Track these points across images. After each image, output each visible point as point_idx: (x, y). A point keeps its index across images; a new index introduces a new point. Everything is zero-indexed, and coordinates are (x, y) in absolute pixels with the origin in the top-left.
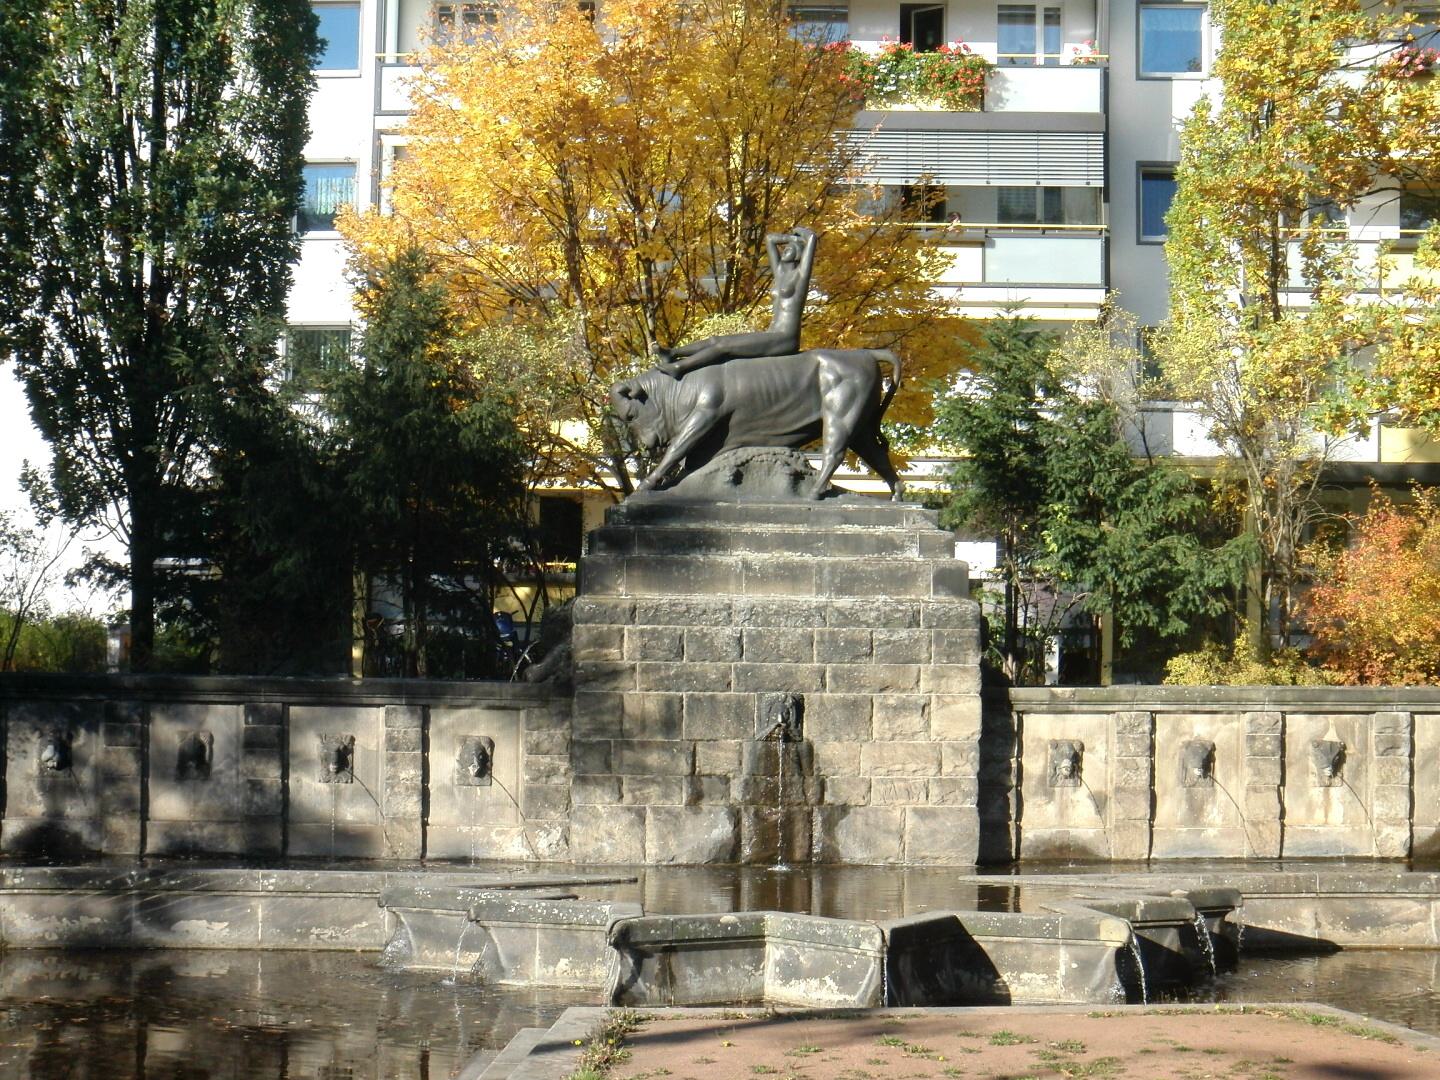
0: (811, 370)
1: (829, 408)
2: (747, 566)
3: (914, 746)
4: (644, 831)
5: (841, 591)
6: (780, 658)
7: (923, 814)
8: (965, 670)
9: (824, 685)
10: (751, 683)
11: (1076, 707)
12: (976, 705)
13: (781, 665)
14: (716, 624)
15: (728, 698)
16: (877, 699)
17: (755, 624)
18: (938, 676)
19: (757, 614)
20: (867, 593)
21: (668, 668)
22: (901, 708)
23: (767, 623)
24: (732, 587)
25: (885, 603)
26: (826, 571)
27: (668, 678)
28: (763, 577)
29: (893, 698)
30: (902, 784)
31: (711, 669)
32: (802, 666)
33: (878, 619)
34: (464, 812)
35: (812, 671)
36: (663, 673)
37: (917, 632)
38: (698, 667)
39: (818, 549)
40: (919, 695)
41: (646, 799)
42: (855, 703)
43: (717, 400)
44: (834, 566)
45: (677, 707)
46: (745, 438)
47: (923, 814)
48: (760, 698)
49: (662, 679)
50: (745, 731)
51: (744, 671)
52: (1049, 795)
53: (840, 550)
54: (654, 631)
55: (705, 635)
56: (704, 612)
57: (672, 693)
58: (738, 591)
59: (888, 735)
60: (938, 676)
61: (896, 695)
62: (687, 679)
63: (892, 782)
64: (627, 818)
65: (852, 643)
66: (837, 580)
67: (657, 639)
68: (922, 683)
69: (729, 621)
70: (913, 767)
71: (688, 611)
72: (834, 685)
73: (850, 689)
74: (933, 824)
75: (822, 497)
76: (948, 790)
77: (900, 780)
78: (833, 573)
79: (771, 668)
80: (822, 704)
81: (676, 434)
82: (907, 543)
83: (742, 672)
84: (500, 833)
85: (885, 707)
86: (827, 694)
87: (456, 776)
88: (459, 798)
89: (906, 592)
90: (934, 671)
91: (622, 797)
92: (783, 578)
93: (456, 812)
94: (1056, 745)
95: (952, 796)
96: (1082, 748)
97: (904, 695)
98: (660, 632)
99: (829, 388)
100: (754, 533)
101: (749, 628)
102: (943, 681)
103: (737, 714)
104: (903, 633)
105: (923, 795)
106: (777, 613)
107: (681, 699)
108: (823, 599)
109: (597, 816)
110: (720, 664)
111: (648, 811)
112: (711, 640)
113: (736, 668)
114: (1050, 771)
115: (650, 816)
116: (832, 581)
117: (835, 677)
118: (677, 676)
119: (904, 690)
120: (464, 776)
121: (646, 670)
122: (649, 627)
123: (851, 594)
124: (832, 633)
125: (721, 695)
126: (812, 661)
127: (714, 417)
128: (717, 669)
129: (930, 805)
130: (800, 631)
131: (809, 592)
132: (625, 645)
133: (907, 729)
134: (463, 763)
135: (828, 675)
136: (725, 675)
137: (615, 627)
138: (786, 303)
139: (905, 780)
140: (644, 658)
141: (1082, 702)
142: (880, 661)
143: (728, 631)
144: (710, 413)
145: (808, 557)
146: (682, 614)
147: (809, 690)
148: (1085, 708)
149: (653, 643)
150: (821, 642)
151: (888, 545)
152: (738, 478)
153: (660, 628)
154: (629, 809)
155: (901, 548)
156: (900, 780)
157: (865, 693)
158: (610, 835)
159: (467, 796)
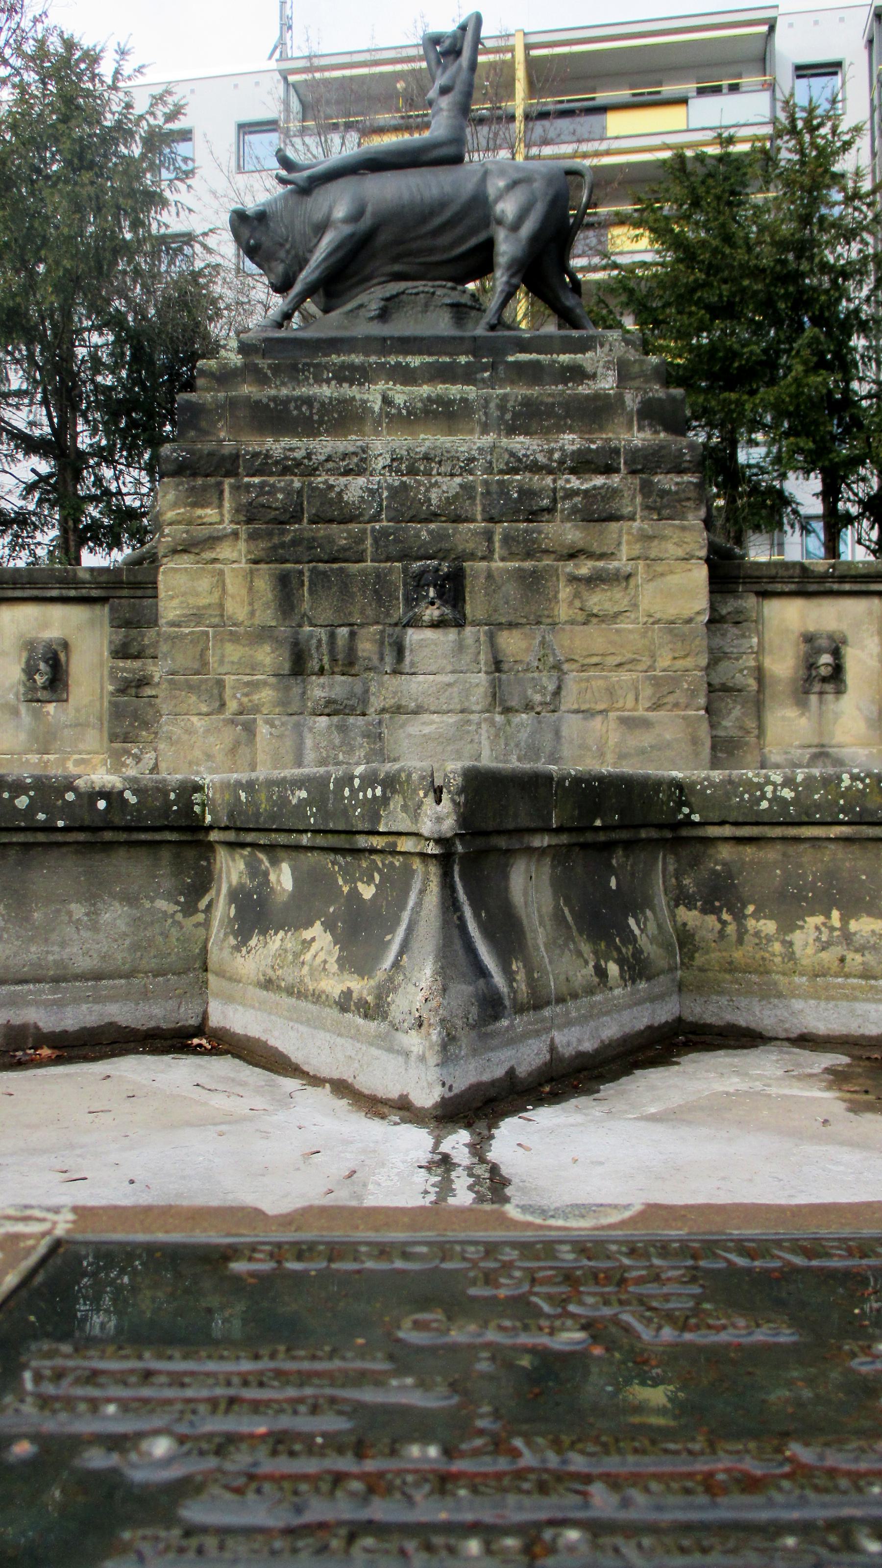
0: (475, 179)
1: (499, 222)
2: (387, 401)
3: (618, 631)
4: (254, 754)
5: (512, 430)
6: (433, 517)
7: (629, 723)
8: (683, 528)
9: (491, 551)
10: (393, 550)
11: (836, 587)
12: (701, 573)
13: (432, 526)
14: (347, 472)
15: (362, 572)
16: (569, 567)
17: (398, 471)
18: (646, 538)
19: (400, 460)
20: (546, 432)
21: (283, 532)
22: (595, 580)
23: (412, 471)
24: (368, 428)
25: (573, 442)
26: (492, 405)
27: (283, 545)
28: (409, 413)
29: (585, 568)
30: (601, 683)
31: (340, 535)
32: (463, 527)
33: (561, 462)
34: (33, 735)
35: (475, 533)
36: (276, 540)
37: (615, 480)
38: (322, 530)
39: (483, 380)
40: (620, 564)
41: (256, 709)
42: (534, 572)
43: (356, 216)
44: (504, 398)
45: (294, 581)
46: (397, 268)
47: (629, 723)
48: (405, 570)
49: (275, 548)
50: (388, 614)
51: (384, 533)
52: (801, 703)
53: (512, 383)
54: (263, 485)
55: (331, 487)
56: (329, 459)
57: (288, 566)
58: (377, 433)
59: (581, 617)
60: (646, 538)
61: (590, 564)
62: (311, 544)
63: (588, 680)
64: (229, 735)
65: (526, 494)
66: (508, 416)
67: (268, 493)
68: (624, 548)
69: (359, 471)
70: (618, 659)
71: (309, 456)
72: (505, 553)
73: (529, 555)
74: (646, 739)
75: (492, 328)
76: (665, 690)
77: (596, 677)
78: (502, 408)
79: (424, 532)
80: (490, 576)
81: (306, 261)
82: (600, 371)
83: (380, 537)
84: (78, 763)
85: (573, 579)
86: (497, 564)
87: (22, 690)
88: (25, 716)
89: (601, 429)
90: (641, 529)
91: (223, 705)
92: (436, 414)
93: (23, 737)
94: (809, 638)
95: (670, 699)
96: (844, 642)
97: (601, 564)
98: (273, 486)
99: (499, 197)
100: (399, 364)
101: (394, 480)
102: (656, 542)
103: (376, 592)
104: (599, 481)
105: (631, 697)
106: (427, 458)
107: (301, 573)
108: (488, 439)
109: (190, 731)
110: (350, 526)
111: (260, 722)
112: (340, 494)
113: (373, 530)
114: (802, 673)
115: (263, 730)
116: (501, 418)
117: (507, 540)
118: (295, 543)
119: (602, 556)
120: (31, 687)
121: (253, 537)
122: (257, 480)
123: (526, 434)
124: (501, 483)
125: (354, 567)
126: (473, 521)
127: (352, 236)
128: (349, 532)
129: (640, 712)
130: (458, 480)
131: (471, 432)
132: (227, 505)
133: (610, 608)
134: (30, 671)
135: (497, 538)
136: (360, 539)
137: (212, 480)
138: (445, 102)
139: (606, 678)
140: (249, 521)
141: (842, 579)
142: (568, 519)
143: (361, 481)
144: (347, 229)
145: (471, 391)
146: (298, 463)
147: (472, 556)
148: (847, 587)
149: (264, 500)
150: (488, 493)
151: (577, 374)
152: (383, 315)
153: (271, 480)
154: (232, 722)
155: (593, 376)
156: (596, 677)
157: (547, 562)
158: (209, 757)
159: (37, 715)
